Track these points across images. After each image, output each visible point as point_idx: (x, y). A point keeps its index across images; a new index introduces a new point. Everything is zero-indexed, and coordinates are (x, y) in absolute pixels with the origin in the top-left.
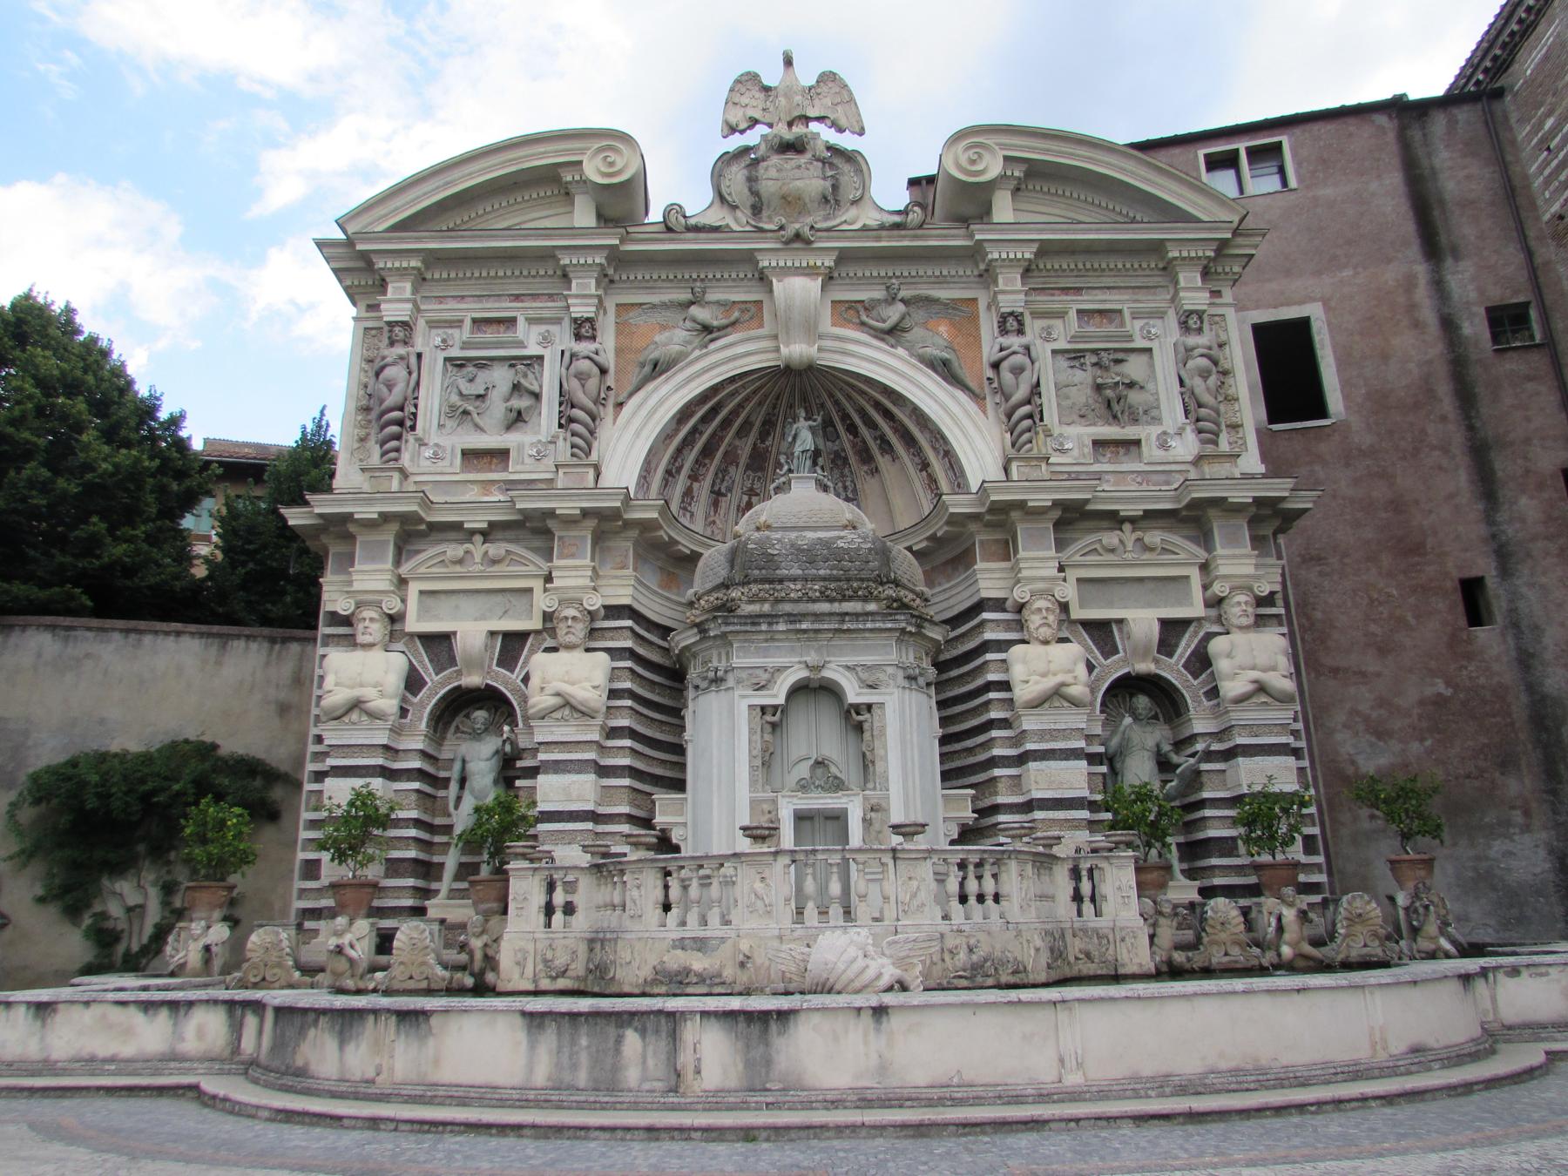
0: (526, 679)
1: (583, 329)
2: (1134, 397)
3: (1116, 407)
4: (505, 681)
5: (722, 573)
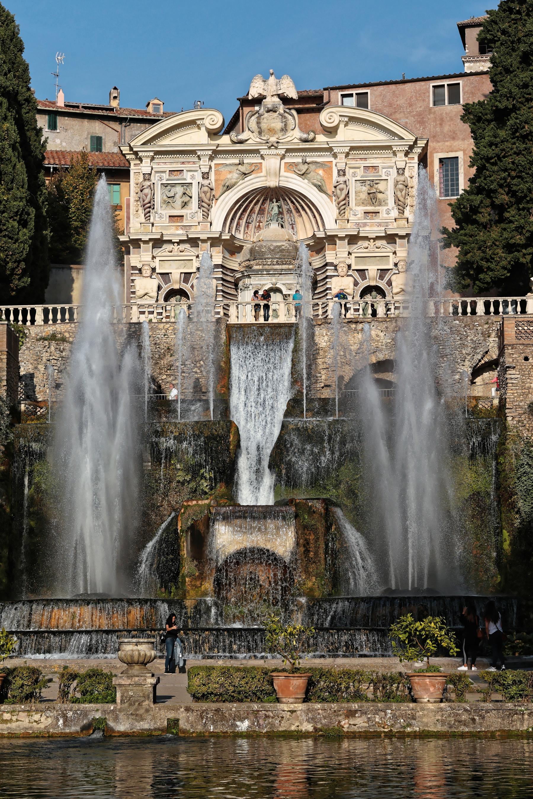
0: (192, 287)
2: (380, 196)
3: (374, 201)
4: (186, 287)
5: (248, 256)
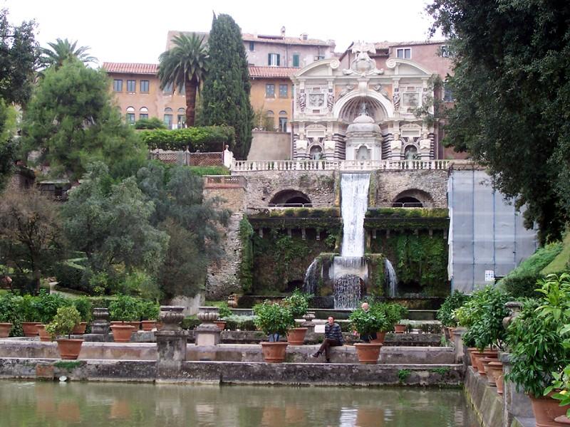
1: (331, 91)
2: (416, 101)
